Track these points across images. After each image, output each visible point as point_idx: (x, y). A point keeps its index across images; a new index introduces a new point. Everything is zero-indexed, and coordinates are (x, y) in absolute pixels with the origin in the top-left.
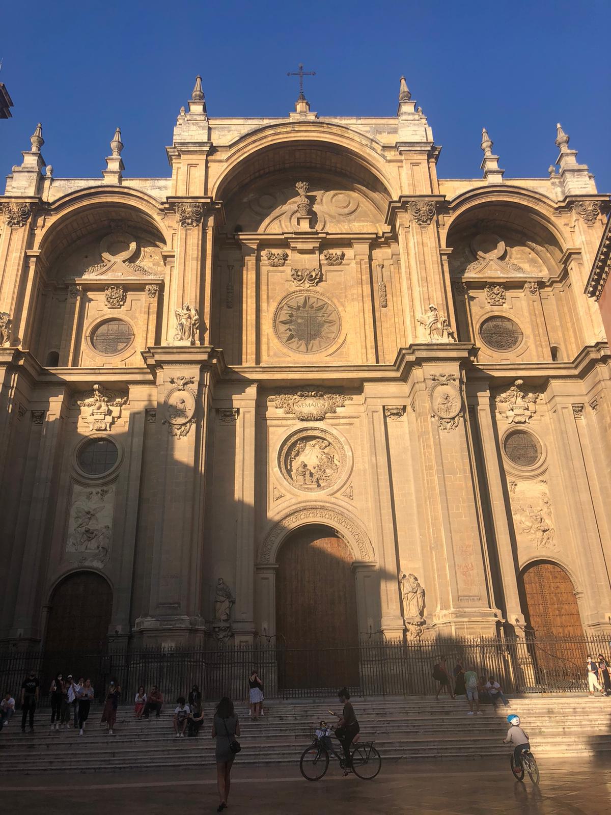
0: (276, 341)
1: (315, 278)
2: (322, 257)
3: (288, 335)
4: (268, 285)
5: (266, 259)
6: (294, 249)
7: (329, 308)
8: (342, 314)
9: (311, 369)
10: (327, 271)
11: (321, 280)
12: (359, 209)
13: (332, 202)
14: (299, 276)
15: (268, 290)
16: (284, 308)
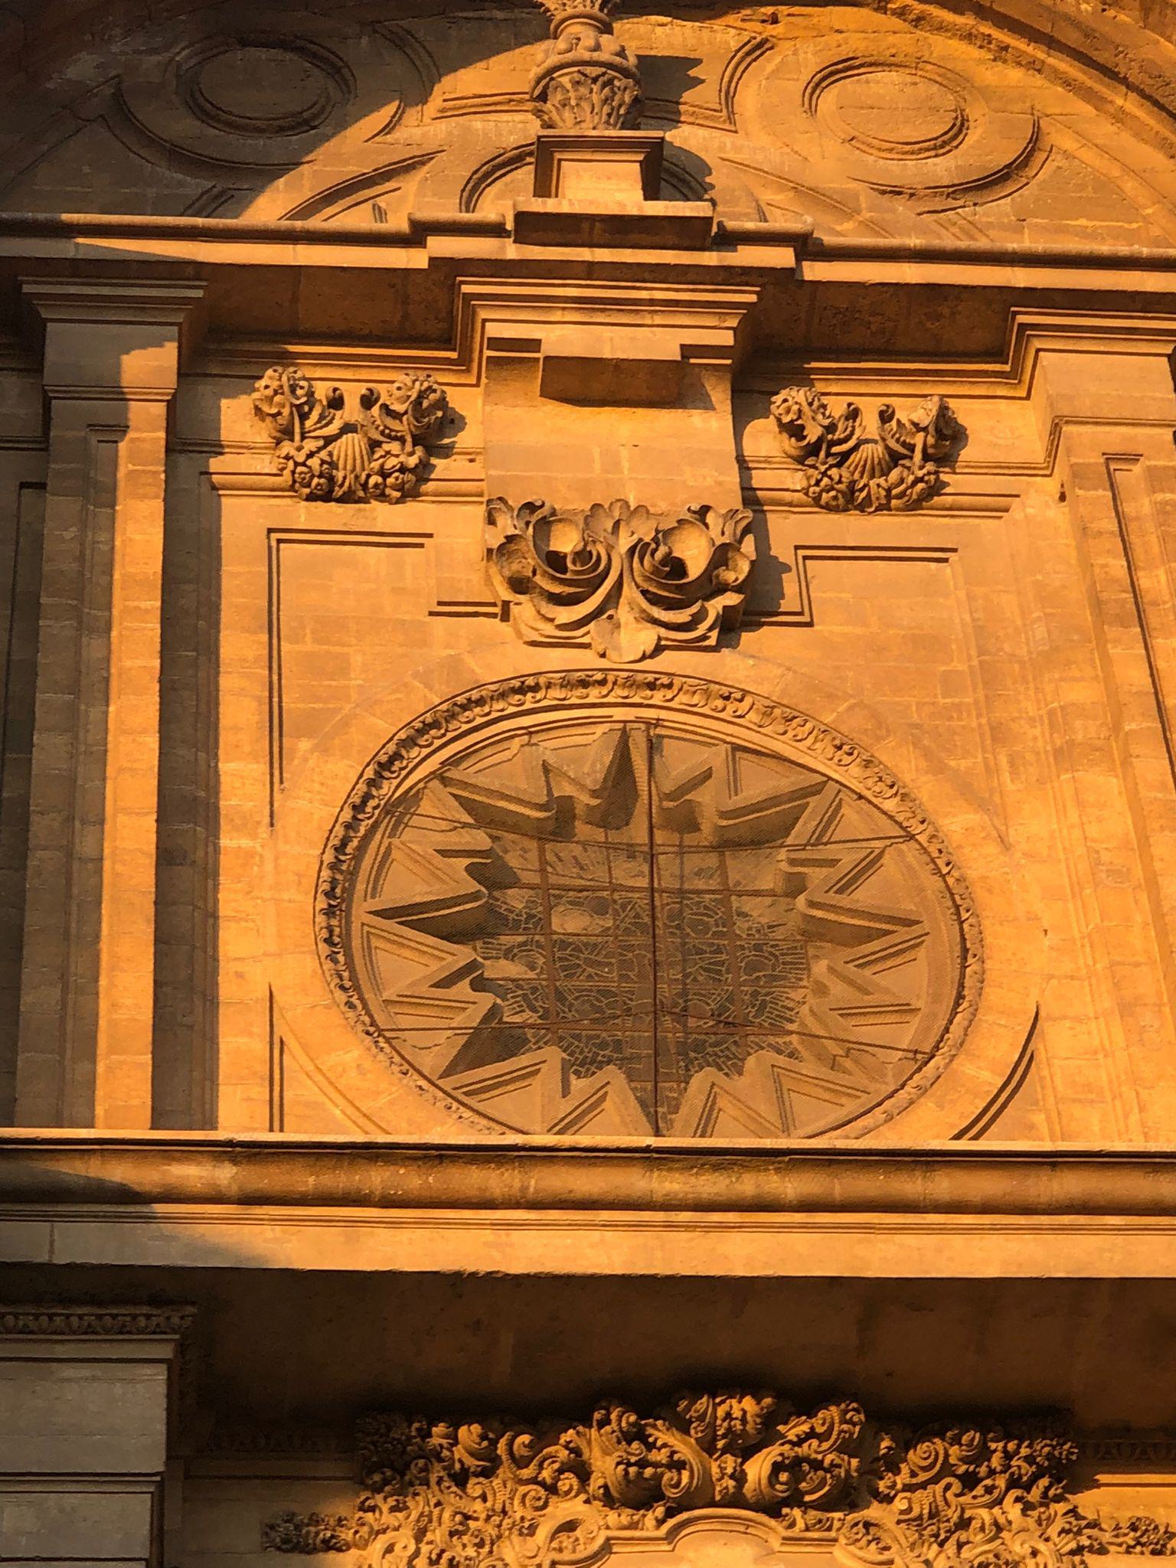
0: (351, 1055)
1: (710, 585)
2: (764, 439)
3: (472, 1017)
4: (272, 628)
5: (262, 433)
6: (513, 357)
7: (853, 820)
8: (979, 863)
9: (748, 1184)
10: (811, 552)
11: (757, 608)
12: (1043, 172)
13: (812, 110)
14: (556, 561)
15: (273, 660)
16: (426, 806)
